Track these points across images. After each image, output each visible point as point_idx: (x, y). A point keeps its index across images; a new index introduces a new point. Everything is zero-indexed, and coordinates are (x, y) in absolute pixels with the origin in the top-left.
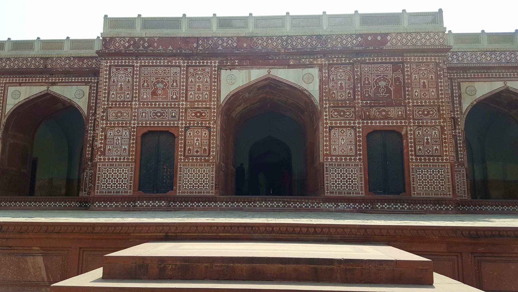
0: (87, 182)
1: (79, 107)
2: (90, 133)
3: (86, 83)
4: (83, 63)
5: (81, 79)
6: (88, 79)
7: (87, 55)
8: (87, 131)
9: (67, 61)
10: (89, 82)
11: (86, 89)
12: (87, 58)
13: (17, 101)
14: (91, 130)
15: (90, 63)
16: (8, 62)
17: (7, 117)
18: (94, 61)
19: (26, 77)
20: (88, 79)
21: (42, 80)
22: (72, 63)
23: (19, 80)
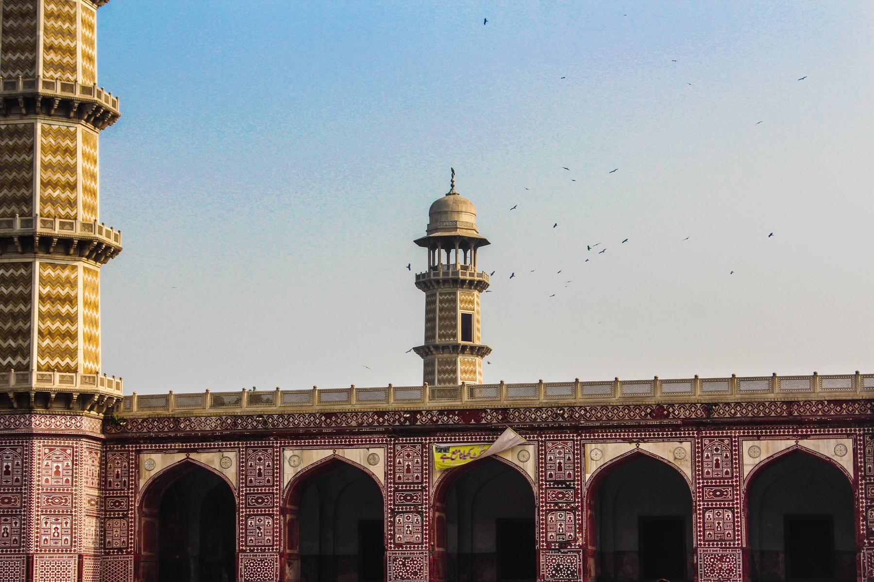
0: (866, 565)
1: (842, 467)
2: (862, 503)
3: (848, 436)
4: (842, 408)
5: (842, 431)
6: (851, 430)
7: (848, 398)
8: (858, 499)
9: (820, 406)
10: (852, 434)
11: (849, 443)
12: (847, 402)
13: (757, 461)
14: (862, 498)
15: (851, 409)
16: (738, 408)
17: (747, 482)
18: (857, 405)
19: (765, 428)
20: (851, 430)
21: (788, 432)
22: (826, 409)
23: (757, 432)
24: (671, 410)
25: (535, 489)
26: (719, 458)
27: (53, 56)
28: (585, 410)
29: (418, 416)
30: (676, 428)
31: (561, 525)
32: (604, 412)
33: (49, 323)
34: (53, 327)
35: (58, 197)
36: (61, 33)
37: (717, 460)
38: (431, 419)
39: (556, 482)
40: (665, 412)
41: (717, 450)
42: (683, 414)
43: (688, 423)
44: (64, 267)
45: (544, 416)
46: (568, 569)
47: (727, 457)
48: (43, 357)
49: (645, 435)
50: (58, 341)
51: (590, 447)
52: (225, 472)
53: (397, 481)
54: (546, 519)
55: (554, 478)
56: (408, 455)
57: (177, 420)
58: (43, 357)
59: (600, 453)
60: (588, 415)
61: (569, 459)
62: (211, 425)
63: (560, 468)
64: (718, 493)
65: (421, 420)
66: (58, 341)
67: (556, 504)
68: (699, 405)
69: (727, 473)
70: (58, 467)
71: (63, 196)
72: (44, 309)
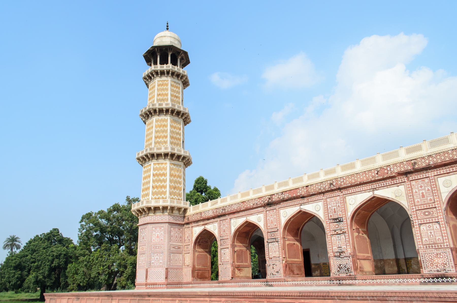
16: (431, 159)
24: (389, 169)
25: (325, 224)
26: (423, 191)
27: (160, 97)
28: (343, 179)
29: (274, 197)
30: (392, 178)
31: (339, 242)
32: (353, 178)
33: (156, 183)
34: (158, 185)
35: (161, 141)
36: (163, 90)
37: (423, 193)
38: (278, 197)
39: (333, 219)
40: (386, 171)
41: (421, 187)
42: (396, 170)
43: (401, 174)
44: (162, 164)
45: (324, 186)
46: (345, 267)
47: (428, 190)
48: (153, 195)
49: (376, 186)
50: (159, 189)
51: (348, 198)
52: (214, 231)
53: (268, 228)
54: (331, 240)
55: (332, 218)
56: (271, 215)
57: (201, 213)
58: (153, 195)
59: (354, 200)
60: (345, 181)
61: (339, 206)
62: (211, 214)
63: (335, 212)
64: (427, 213)
65: (275, 199)
66: (159, 189)
67: (335, 231)
68: (405, 163)
69: (431, 200)
70: (158, 235)
71: (162, 140)
72: (154, 179)
